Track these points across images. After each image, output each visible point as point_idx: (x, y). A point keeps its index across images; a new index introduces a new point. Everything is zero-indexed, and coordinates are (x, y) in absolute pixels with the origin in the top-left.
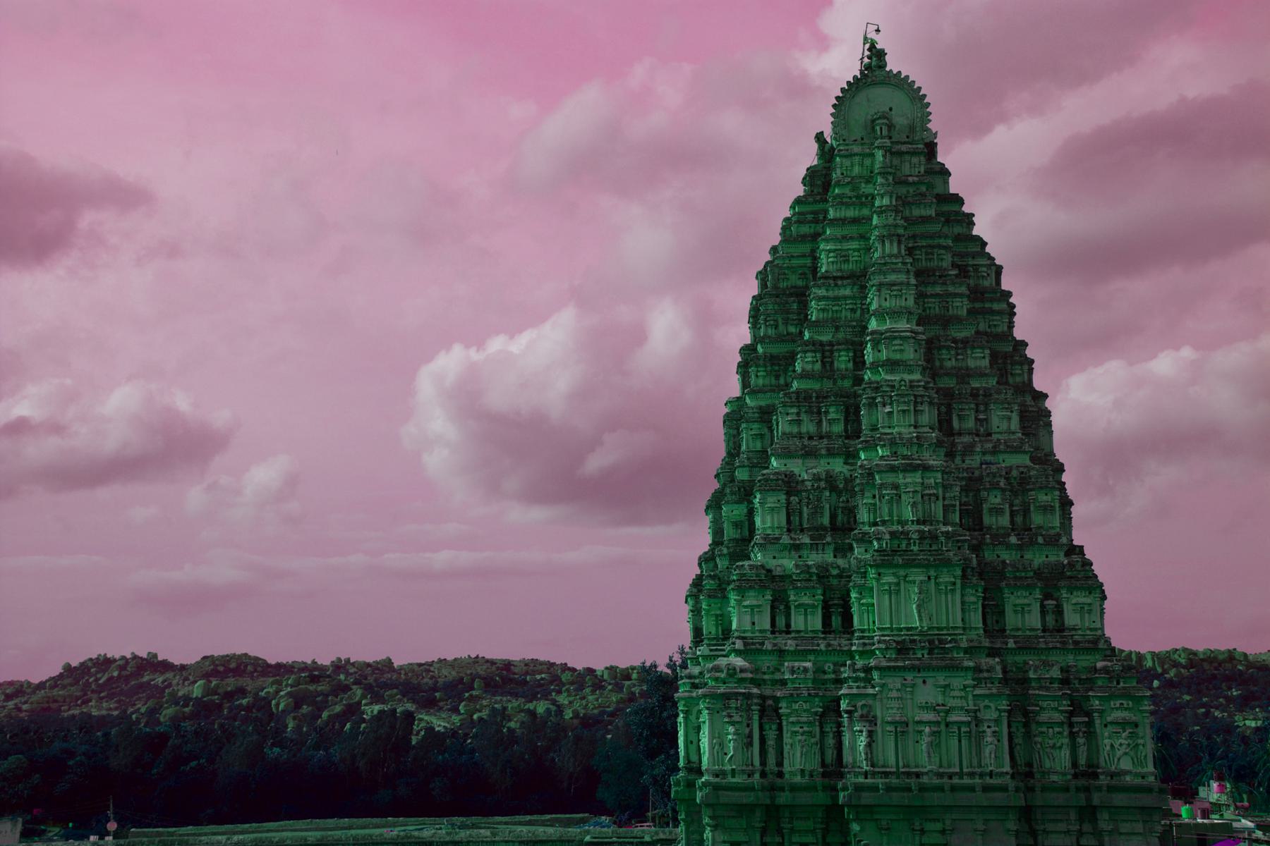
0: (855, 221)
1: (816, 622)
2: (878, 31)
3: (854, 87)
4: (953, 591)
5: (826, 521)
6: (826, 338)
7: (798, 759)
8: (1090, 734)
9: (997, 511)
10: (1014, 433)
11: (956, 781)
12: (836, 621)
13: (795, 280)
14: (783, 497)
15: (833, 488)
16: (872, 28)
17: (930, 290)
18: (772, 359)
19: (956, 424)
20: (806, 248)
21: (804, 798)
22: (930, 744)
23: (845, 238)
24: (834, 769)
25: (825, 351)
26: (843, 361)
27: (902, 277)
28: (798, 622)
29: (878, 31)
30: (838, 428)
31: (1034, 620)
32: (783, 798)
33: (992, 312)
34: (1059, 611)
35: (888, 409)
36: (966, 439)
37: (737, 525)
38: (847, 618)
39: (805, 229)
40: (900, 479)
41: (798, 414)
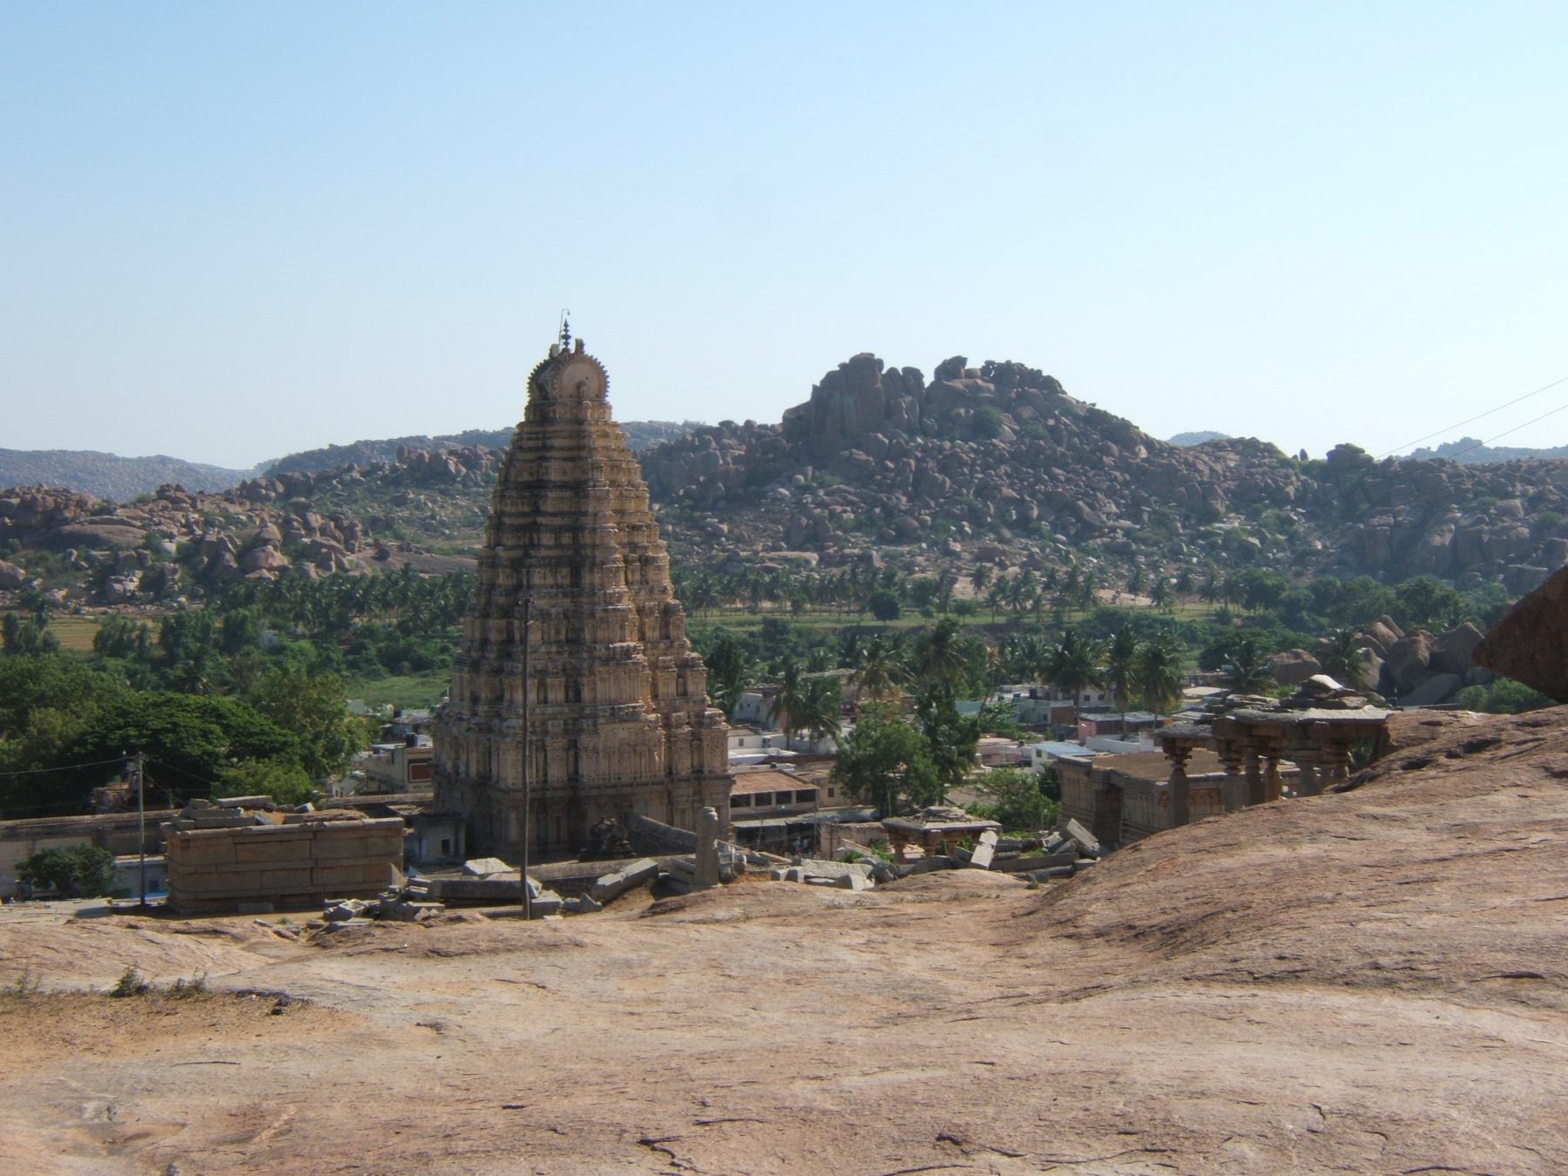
0: (571, 449)
1: (561, 696)
5: (563, 637)
6: (557, 521)
7: (557, 772)
8: (700, 748)
12: (571, 694)
13: (526, 477)
15: (566, 616)
18: (518, 529)
20: (532, 456)
21: (560, 793)
23: (565, 459)
24: (574, 778)
25: (557, 531)
26: (566, 539)
28: (551, 696)
30: (567, 581)
31: (672, 689)
32: (549, 794)
34: (685, 684)
37: (500, 631)
38: (578, 693)
39: (531, 444)
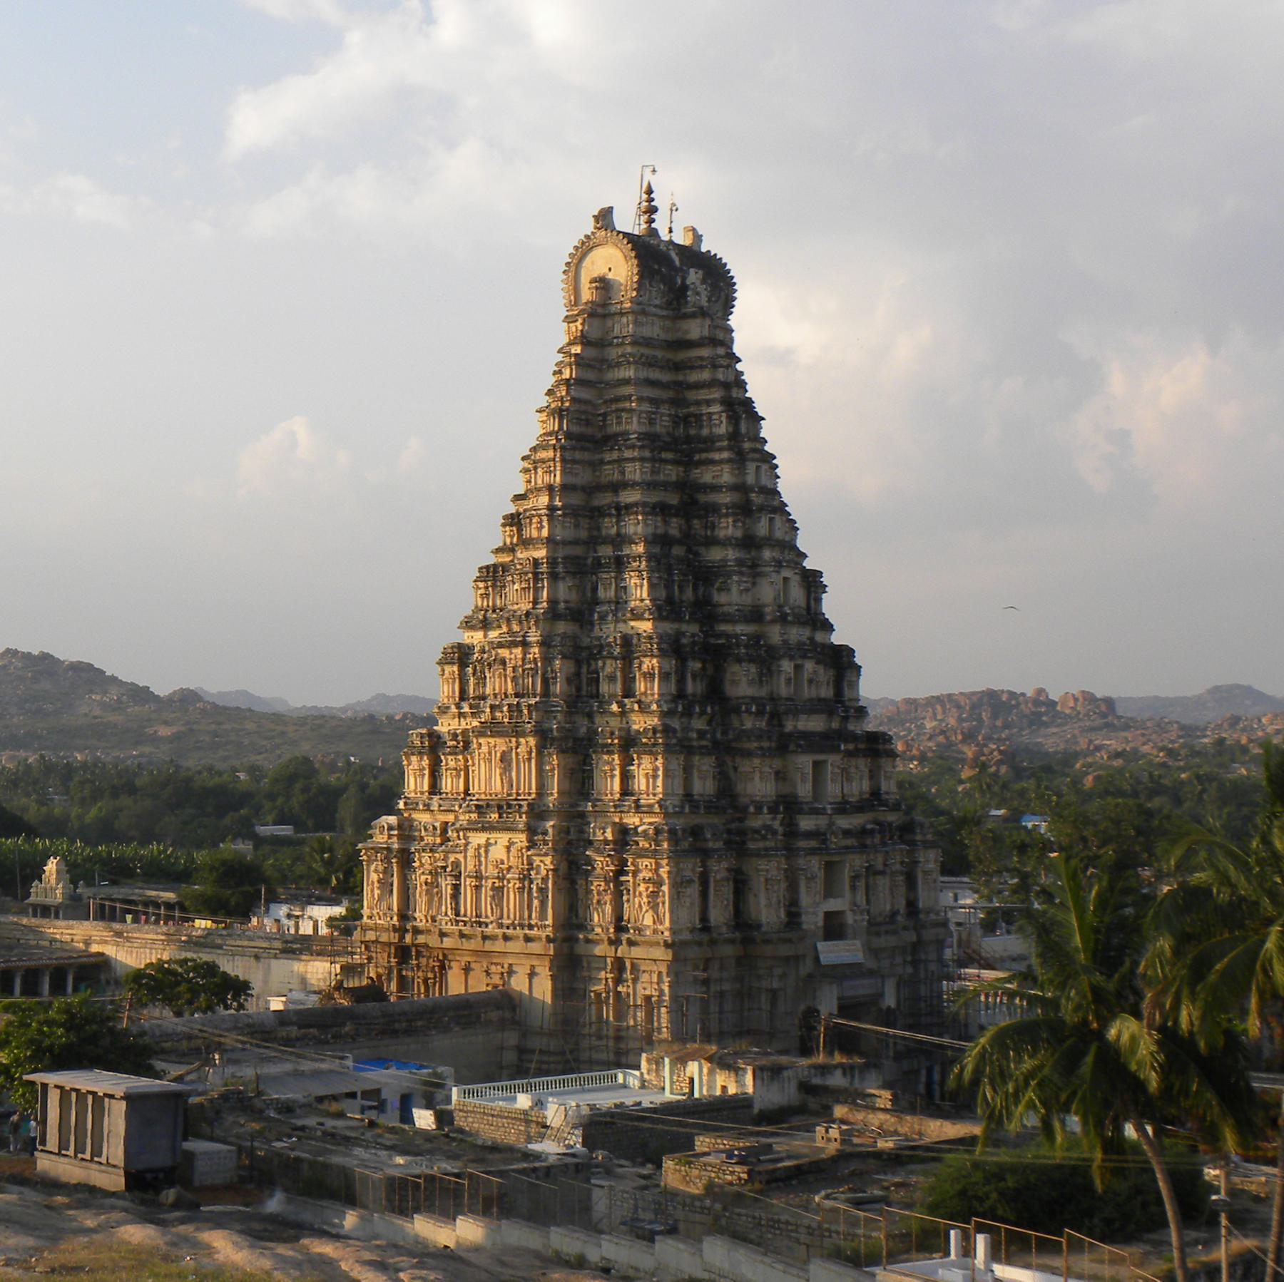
2: (654, 171)
3: (585, 248)
4: (529, 759)
9: (612, 678)
10: (642, 600)
11: (510, 932)
14: (455, 668)
16: (649, 170)
17: (608, 457)
19: (601, 593)
22: (493, 897)
27: (550, 454)
29: (654, 171)
33: (712, 462)
35: (516, 586)
36: (605, 608)
40: (504, 653)
41: (487, 588)
